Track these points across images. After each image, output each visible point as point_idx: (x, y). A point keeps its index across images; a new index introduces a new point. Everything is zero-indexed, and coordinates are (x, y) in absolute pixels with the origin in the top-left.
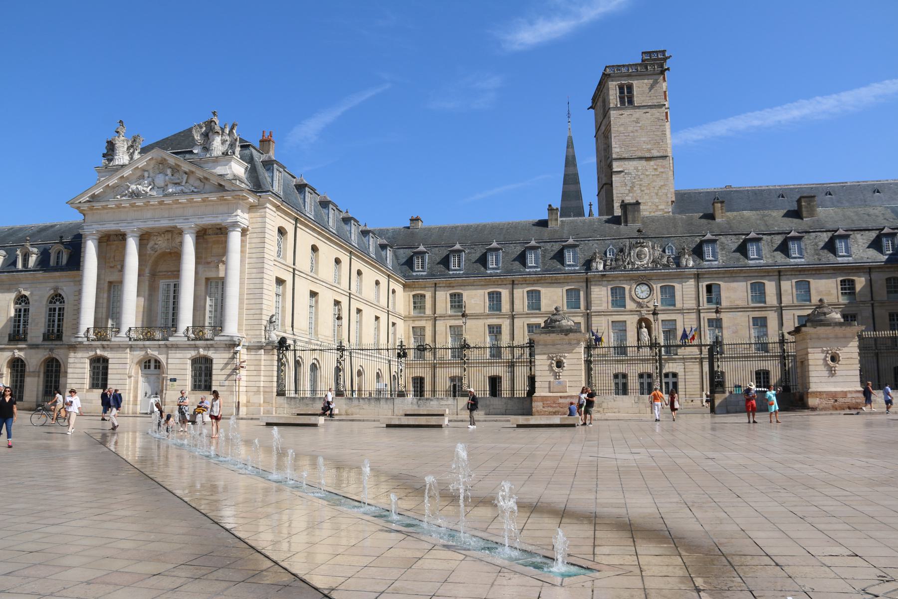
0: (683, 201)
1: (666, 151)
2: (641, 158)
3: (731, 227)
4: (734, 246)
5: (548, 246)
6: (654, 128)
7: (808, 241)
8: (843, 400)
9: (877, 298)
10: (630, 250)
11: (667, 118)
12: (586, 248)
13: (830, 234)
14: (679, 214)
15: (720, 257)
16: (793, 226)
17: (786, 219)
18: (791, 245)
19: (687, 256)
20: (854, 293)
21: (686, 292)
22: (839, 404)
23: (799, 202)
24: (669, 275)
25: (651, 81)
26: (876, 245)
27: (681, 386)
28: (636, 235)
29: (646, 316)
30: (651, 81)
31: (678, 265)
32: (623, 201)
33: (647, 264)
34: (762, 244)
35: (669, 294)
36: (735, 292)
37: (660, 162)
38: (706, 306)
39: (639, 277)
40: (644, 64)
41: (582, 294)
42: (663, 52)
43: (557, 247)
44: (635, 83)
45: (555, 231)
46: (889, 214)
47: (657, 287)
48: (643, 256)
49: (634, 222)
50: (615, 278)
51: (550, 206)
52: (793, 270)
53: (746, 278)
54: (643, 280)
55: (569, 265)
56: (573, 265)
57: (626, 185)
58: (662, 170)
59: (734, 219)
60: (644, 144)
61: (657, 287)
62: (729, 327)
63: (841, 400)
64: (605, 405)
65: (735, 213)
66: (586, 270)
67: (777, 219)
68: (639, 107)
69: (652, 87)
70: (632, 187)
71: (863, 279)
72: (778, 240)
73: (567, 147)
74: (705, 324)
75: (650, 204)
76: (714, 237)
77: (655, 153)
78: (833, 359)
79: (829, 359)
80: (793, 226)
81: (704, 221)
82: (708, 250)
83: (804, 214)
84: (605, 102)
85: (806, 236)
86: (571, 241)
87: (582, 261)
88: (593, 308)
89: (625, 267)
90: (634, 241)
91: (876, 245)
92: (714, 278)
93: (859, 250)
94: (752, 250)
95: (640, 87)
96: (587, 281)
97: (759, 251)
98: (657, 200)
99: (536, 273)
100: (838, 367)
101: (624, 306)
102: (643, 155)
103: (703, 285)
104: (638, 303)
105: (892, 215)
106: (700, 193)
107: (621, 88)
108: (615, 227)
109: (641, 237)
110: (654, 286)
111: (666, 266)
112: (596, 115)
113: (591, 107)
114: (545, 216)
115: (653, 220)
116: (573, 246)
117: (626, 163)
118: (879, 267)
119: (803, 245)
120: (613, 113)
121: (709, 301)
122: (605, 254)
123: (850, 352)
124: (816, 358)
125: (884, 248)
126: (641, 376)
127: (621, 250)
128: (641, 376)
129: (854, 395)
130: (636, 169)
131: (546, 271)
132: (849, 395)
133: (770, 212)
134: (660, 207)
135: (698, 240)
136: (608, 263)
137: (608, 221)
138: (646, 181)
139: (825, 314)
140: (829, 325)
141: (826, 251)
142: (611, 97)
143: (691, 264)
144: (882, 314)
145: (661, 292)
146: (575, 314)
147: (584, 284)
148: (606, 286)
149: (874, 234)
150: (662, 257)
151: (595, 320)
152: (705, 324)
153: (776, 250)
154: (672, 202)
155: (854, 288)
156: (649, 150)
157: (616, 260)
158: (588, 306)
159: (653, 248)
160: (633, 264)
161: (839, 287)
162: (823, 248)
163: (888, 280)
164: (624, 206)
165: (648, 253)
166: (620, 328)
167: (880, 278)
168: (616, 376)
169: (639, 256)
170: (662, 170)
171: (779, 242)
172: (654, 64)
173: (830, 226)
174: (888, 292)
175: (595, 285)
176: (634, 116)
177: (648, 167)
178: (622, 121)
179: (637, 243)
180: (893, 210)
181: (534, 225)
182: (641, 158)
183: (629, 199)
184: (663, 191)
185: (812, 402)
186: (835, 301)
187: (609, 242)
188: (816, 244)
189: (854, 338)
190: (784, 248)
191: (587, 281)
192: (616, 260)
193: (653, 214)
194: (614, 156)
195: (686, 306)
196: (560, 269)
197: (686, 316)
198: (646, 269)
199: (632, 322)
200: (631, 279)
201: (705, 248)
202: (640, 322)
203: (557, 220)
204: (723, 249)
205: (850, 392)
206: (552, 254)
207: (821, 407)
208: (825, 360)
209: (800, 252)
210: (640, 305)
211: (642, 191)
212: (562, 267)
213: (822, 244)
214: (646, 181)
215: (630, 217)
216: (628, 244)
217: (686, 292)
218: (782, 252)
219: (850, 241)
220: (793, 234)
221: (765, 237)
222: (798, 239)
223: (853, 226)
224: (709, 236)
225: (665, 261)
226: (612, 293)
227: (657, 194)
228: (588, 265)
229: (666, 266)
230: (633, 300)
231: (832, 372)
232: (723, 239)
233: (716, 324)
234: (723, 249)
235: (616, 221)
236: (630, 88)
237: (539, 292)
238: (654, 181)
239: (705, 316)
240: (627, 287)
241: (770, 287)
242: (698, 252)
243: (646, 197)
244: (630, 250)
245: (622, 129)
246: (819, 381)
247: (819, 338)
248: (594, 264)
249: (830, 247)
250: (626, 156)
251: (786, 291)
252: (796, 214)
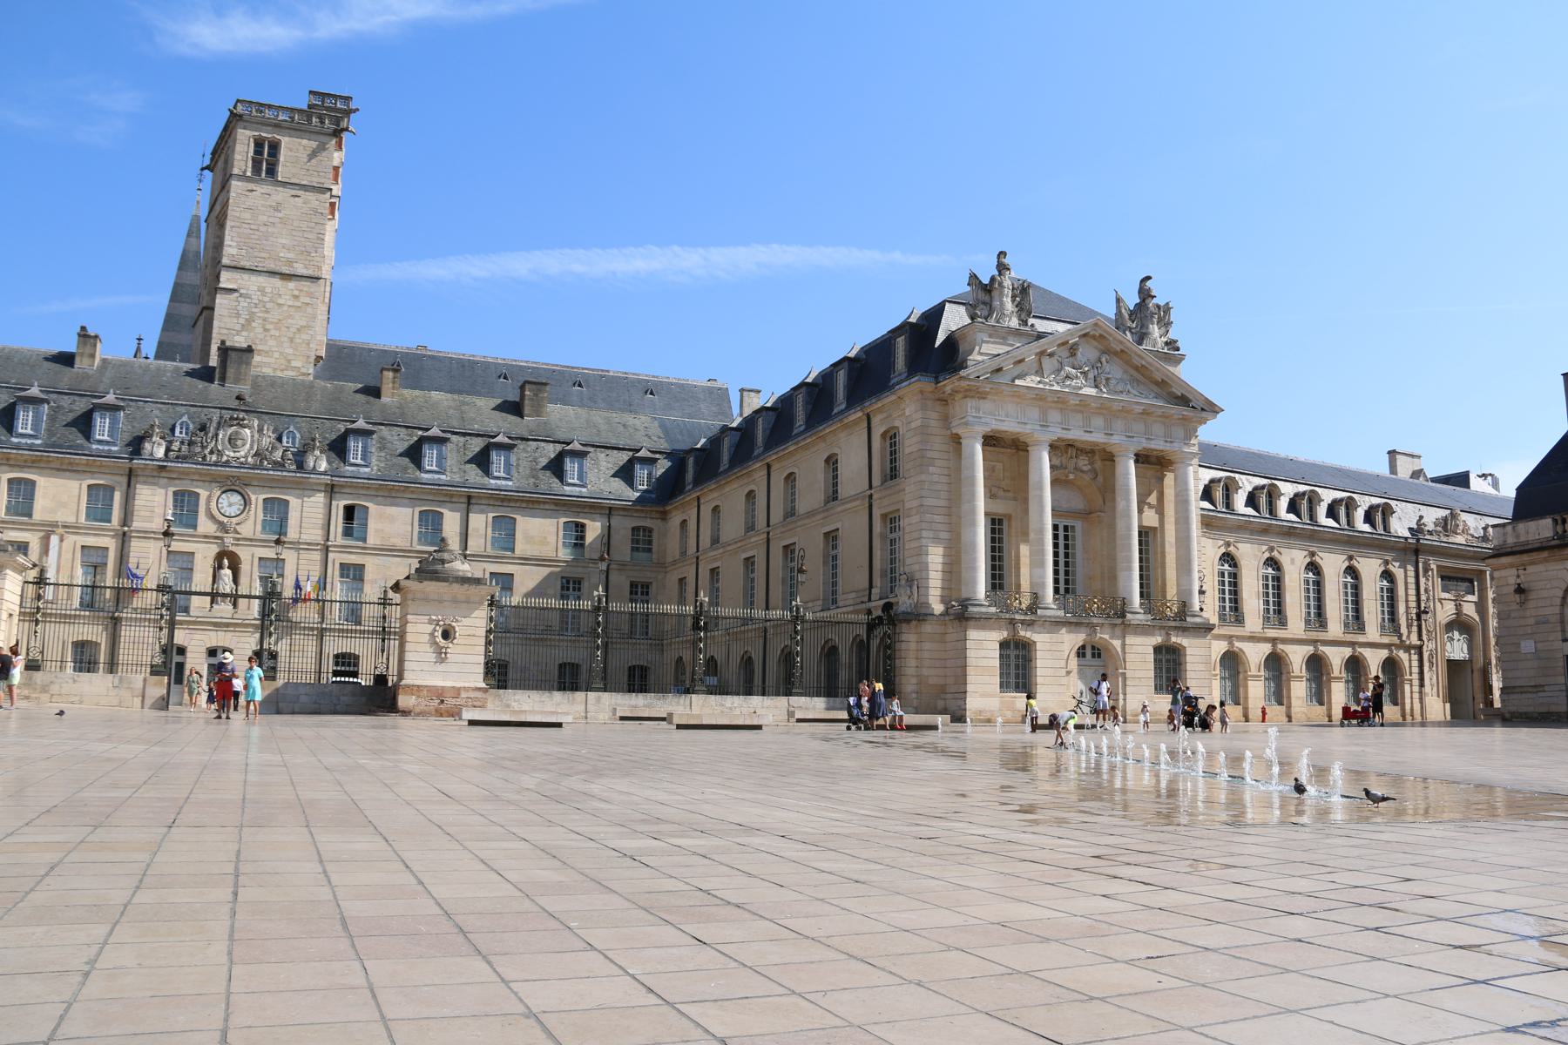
0: (339, 359)
1: (320, 268)
2: (273, 273)
3: (403, 414)
4: (402, 447)
5: (65, 401)
6: (304, 225)
7: (522, 453)
8: (454, 701)
9: (616, 556)
10: (218, 429)
11: (332, 213)
12: (139, 414)
13: (559, 447)
14: (331, 378)
15: (374, 460)
16: (504, 426)
17: (497, 413)
18: (494, 455)
19: (317, 453)
20: (582, 545)
21: (309, 514)
22: (444, 705)
23: (522, 388)
24: (283, 480)
25: (314, 144)
26: (626, 473)
28: (234, 404)
29: (232, 548)
30: (314, 144)
31: (301, 466)
32: (223, 342)
33: (246, 457)
34: (448, 449)
35: (277, 515)
36: (392, 523)
37: (306, 285)
38: (340, 540)
39: (228, 477)
40: (307, 113)
41: (117, 496)
42: (347, 99)
43: (81, 406)
44: (286, 142)
45: (86, 376)
46: (655, 429)
47: (258, 499)
48: (239, 443)
49: (237, 381)
50: (183, 475)
51: (83, 328)
52: (491, 497)
53: (413, 502)
54: (234, 484)
55: (100, 442)
56: (107, 443)
57: (238, 315)
58: (307, 300)
59: (413, 401)
60: (282, 249)
61: (258, 499)
62: (374, 582)
63: (450, 701)
64: (55, 689)
65: (417, 393)
66: (132, 453)
67: (482, 412)
68: (285, 184)
69: (313, 154)
70: (249, 321)
71: (598, 524)
72: (476, 445)
73: (189, 235)
74: (334, 572)
75: (276, 355)
76: (370, 427)
77: (300, 269)
78: (446, 635)
79: (439, 634)
80: (504, 426)
81: (361, 397)
82: (355, 446)
83: (527, 410)
84: (228, 163)
85: (521, 445)
86: (110, 398)
87: (127, 437)
88: (136, 525)
89: (204, 458)
90: (227, 415)
91: (626, 473)
92: (359, 496)
93: (597, 477)
94: (430, 456)
95: (293, 150)
96: (131, 474)
97: (441, 459)
98: (290, 351)
99: (31, 448)
100: (452, 648)
101: (195, 527)
102: (277, 269)
103: (340, 505)
104: (221, 523)
105: (659, 432)
106: (371, 350)
107: (259, 144)
108: (201, 384)
109: (241, 410)
110: (253, 497)
111: (279, 465)
112: (214, 182)
113: (207, 168)
114: (70, 345)
115: (273, 382)
116: (114, 408)
117: (246, 276)
118: (624, 509)
119: (513, 458)
120: (236, 186)
121: (348, 533)
122: (173, 430)
123: (474, 625)
124: (419, 630)
125: (637, 481)
126: (212, 652)
127: (203, 428)
128: (212, 652)
129: (472, 694)
130: (262, 290)
131: (51, 446)
132: (463, 695)
133: (474, 399)
134: (294, 364)
135: (342, 427)
136: (176, 446)
137: (191, 374)
138: (275, 315)
139: (443, 562)
140: (445, 580)
141: (548, 473)
142: (237, 157)
143: (323, 466)
144: (621, 581)
145: (265, 509)
146: (98, 532)
147: (124, 480)
148: (165, 487)
149: (624, 457)
150: (274, 448)
151: (136, 547)
152: (334, 572)
153: (469, 462)
154: (319, 358)
155: (583, 538)
156: (290, 262)
157: (191, 443)
158: (126, 519)
159: (260, 430)
160: (220, 454)
161: (561, 533)
162: (545, 468)
163: (635, 530)
164: (225, 351)
165: (250, 439)
166: (184, 563)
167: (623, 526)
169: (232, 441)
170: (307, 300)
171: (477, 449)
172: (328, 117)
173: (561, 436)
174: (633, 549)
175: (145, 483)
176: (274, 197)
178: (250, 202)
179: (232, 418)
180: (662, 425)
181: (47, 359)
182: (273, 273)
183: (240, 341)
184: (305, 337)
185: (403, 701)
186: (552, 555)
187: (183, 409)
188: (535, 460)
189: (481, 603)
190: (482, 461)
191: (131, 474)
192: (191, 443)
193: (279, 374)
194: (225, 261)
195: (305, 538)
196: (81, 447)
197: (304, 554)
198: (242, 466)
199: (204, 556)
200: (213, 480)
201: (351, 444)
202: (220, 557)
203: (93, 356)
204: (381, 449)
205: (466, 689)
206: (71, 417)
207: (417, 710)
208: (432, 635)
209: (507, 471)
210: (223, 527)
211: (266, 330)
212: (86, 443)
213: (544, 462)
214: (275, 315)
215: (231, 372)
216: (215, 419)
217: (309, 514)
218: (479, 466)
219: (587, 463)
220: (500, 439)
221: (454, 438)
222: (507, 448)
223: (596, 440)
224: (361, 424)
225: (278, 455)
226: (175, 501)
227: (291, 340)
228: (136, 445)
229: (279, 465)
230: (212, 517)
231: (441, 655)
232: (384, 430)
233: (354, 573)
234: (381, 449)
235: (206, 374)
236: (275, 147)
237: (33, 483)
238: (290, 317)
239: (336, 558)
240: (203, 494)
241: (451, 522)
242: (338, 448)
243: (272, 342)
244: (218, 429)
245: (247, 215)
246: (421, 670)
247: (426, 600)
248: (147, 446)
249: (556, 467)
250: (244, 263)
251: (477, 530)
252: (514, 408)
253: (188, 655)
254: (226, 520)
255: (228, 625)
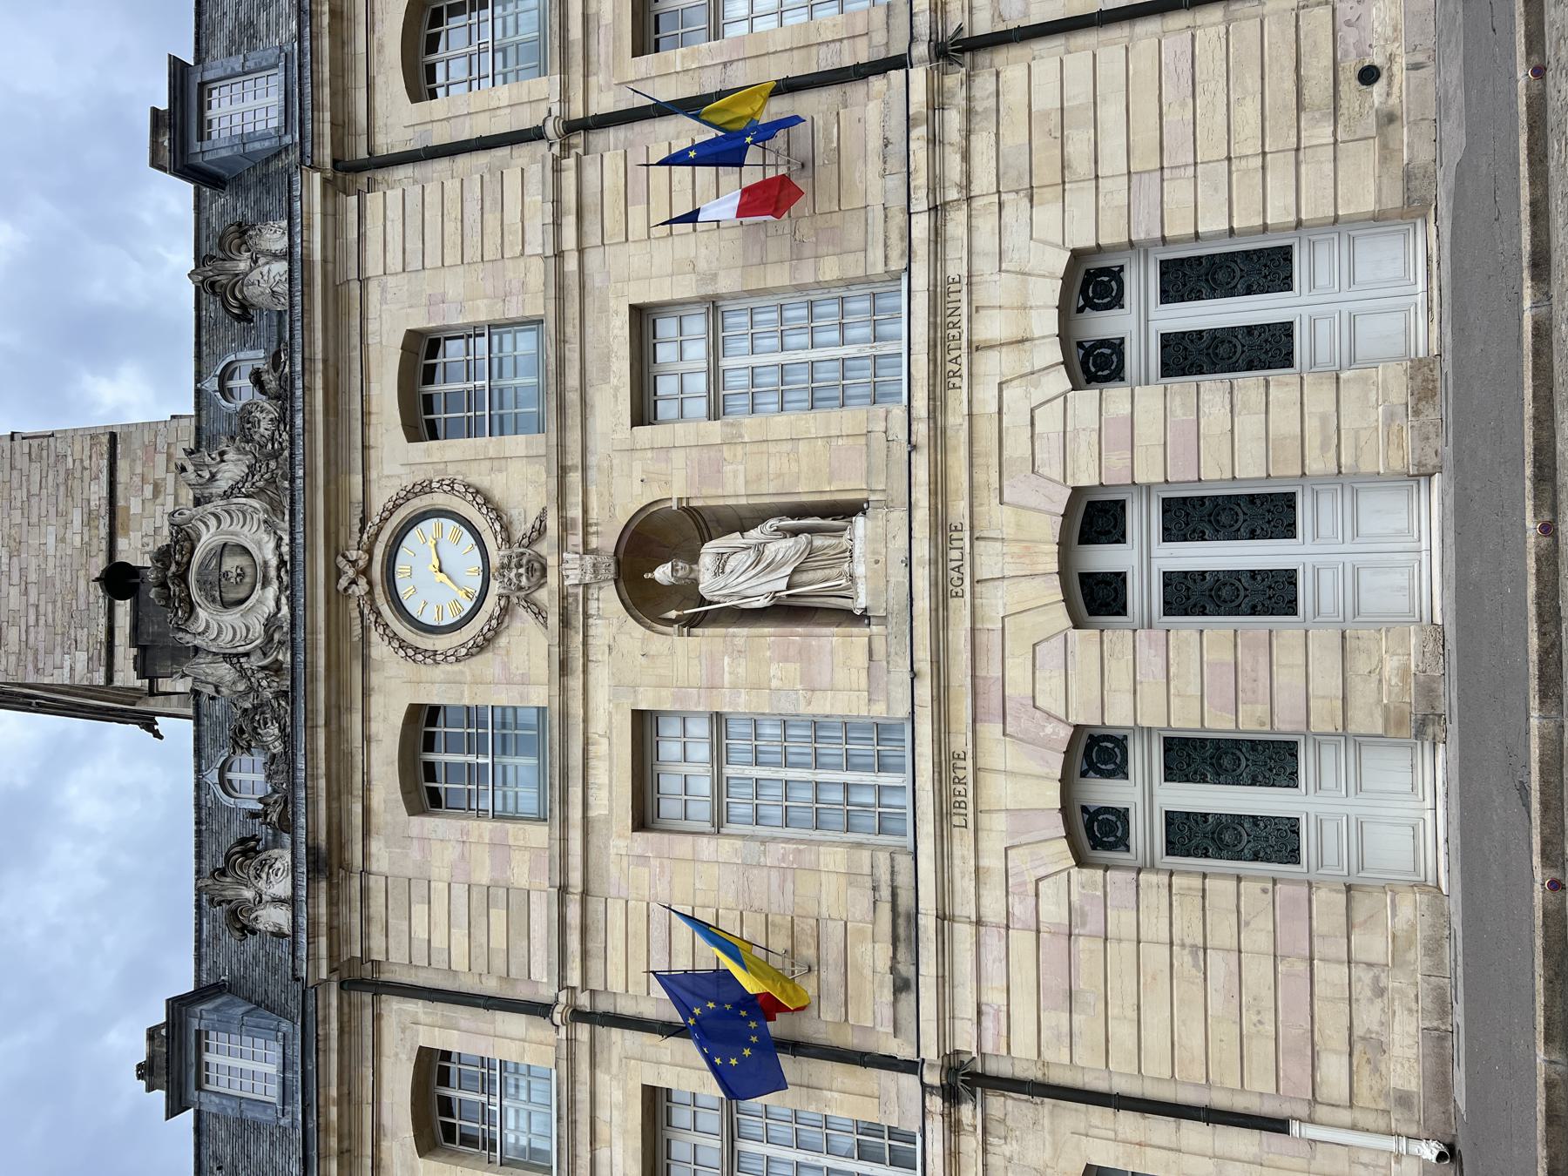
27: (1205, 215)
58: (161, 459)
77: (99, 491)
102: (104, 546)
126: (1098, 598)
147: (396, 1010)
156: (89, 520)
168: (1096, 834)
177: (147, 526)
202: (644, 601)
253: (1118, 717)
254: (495, 587)
255: (941, 527)
